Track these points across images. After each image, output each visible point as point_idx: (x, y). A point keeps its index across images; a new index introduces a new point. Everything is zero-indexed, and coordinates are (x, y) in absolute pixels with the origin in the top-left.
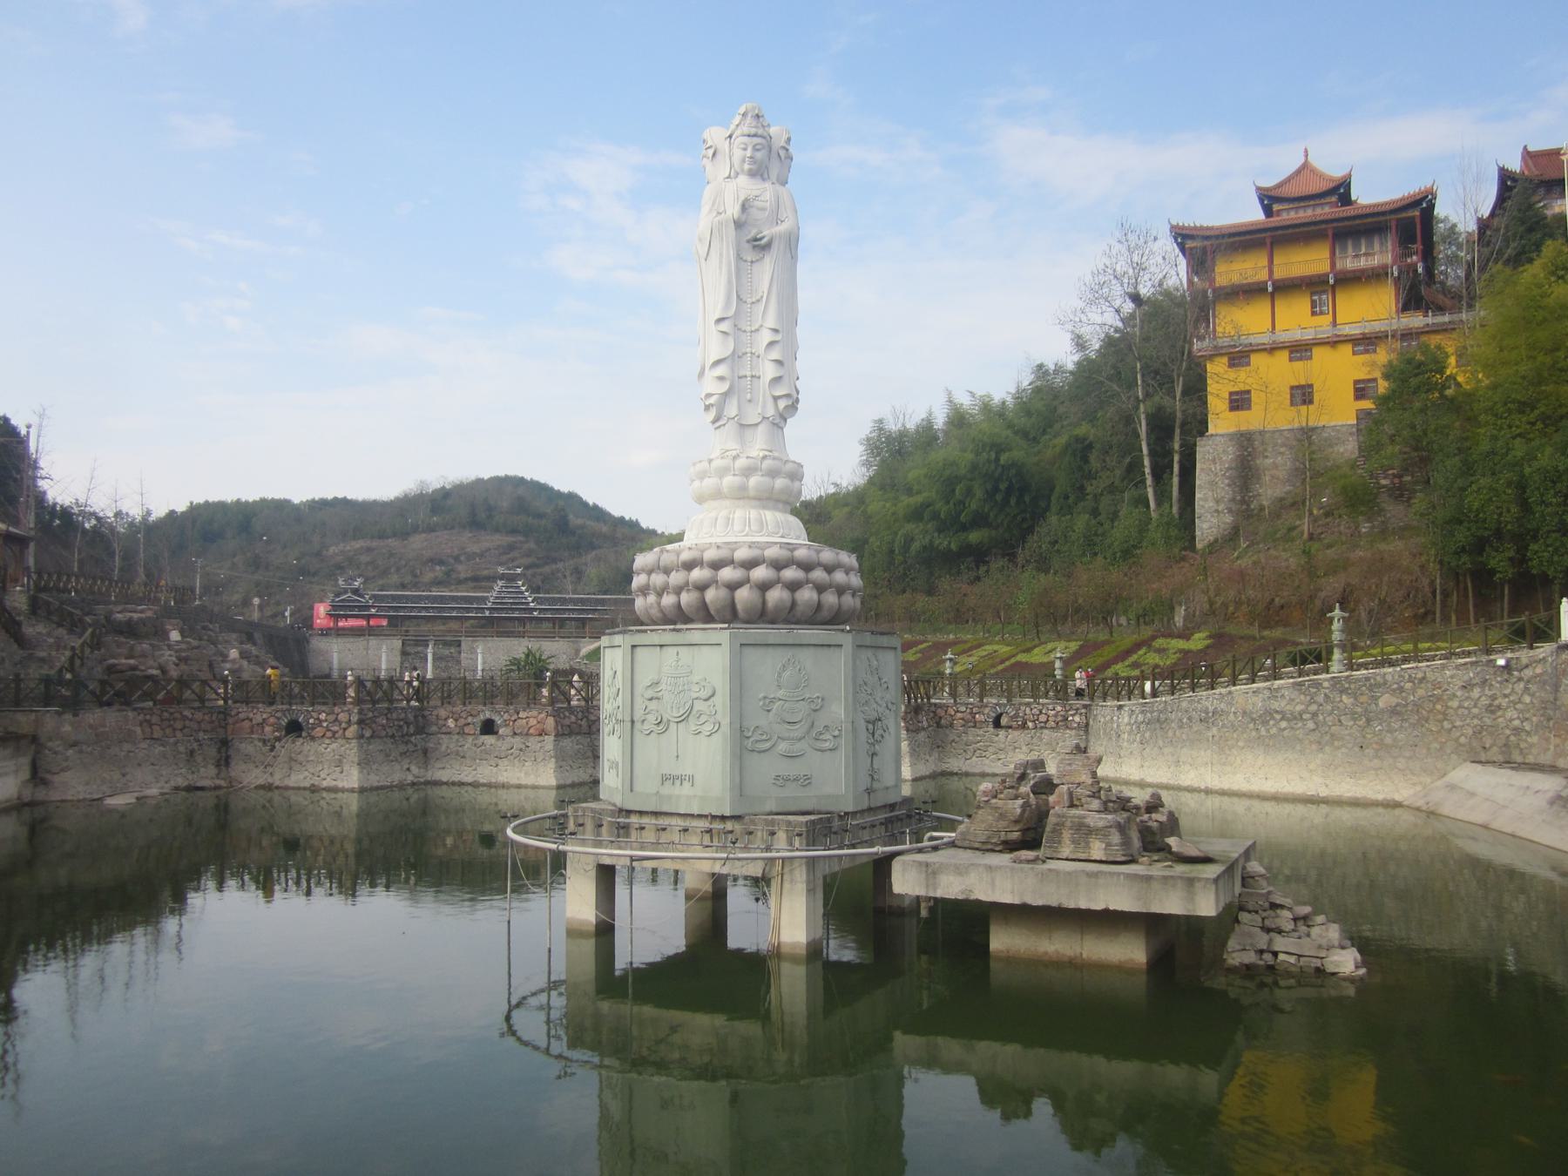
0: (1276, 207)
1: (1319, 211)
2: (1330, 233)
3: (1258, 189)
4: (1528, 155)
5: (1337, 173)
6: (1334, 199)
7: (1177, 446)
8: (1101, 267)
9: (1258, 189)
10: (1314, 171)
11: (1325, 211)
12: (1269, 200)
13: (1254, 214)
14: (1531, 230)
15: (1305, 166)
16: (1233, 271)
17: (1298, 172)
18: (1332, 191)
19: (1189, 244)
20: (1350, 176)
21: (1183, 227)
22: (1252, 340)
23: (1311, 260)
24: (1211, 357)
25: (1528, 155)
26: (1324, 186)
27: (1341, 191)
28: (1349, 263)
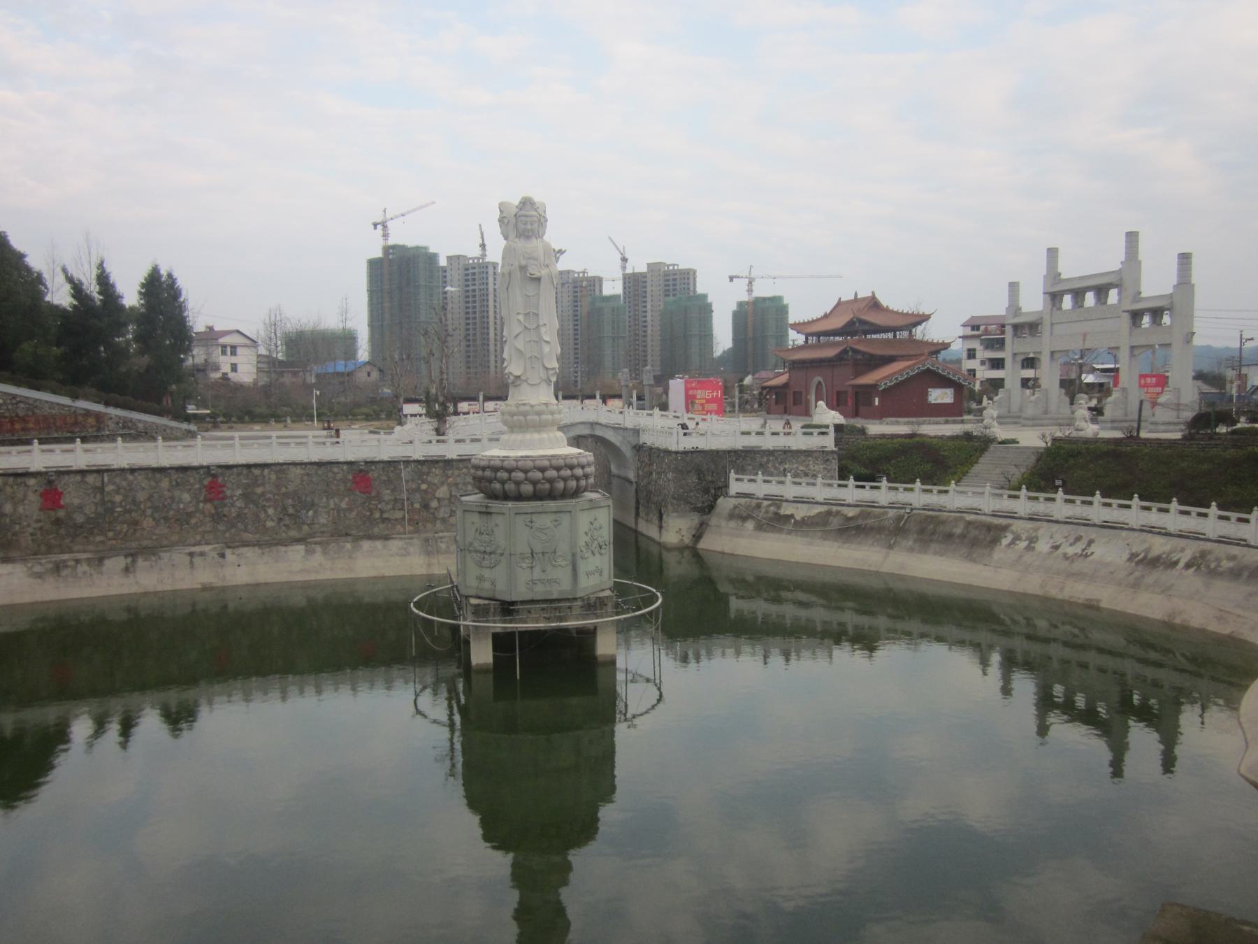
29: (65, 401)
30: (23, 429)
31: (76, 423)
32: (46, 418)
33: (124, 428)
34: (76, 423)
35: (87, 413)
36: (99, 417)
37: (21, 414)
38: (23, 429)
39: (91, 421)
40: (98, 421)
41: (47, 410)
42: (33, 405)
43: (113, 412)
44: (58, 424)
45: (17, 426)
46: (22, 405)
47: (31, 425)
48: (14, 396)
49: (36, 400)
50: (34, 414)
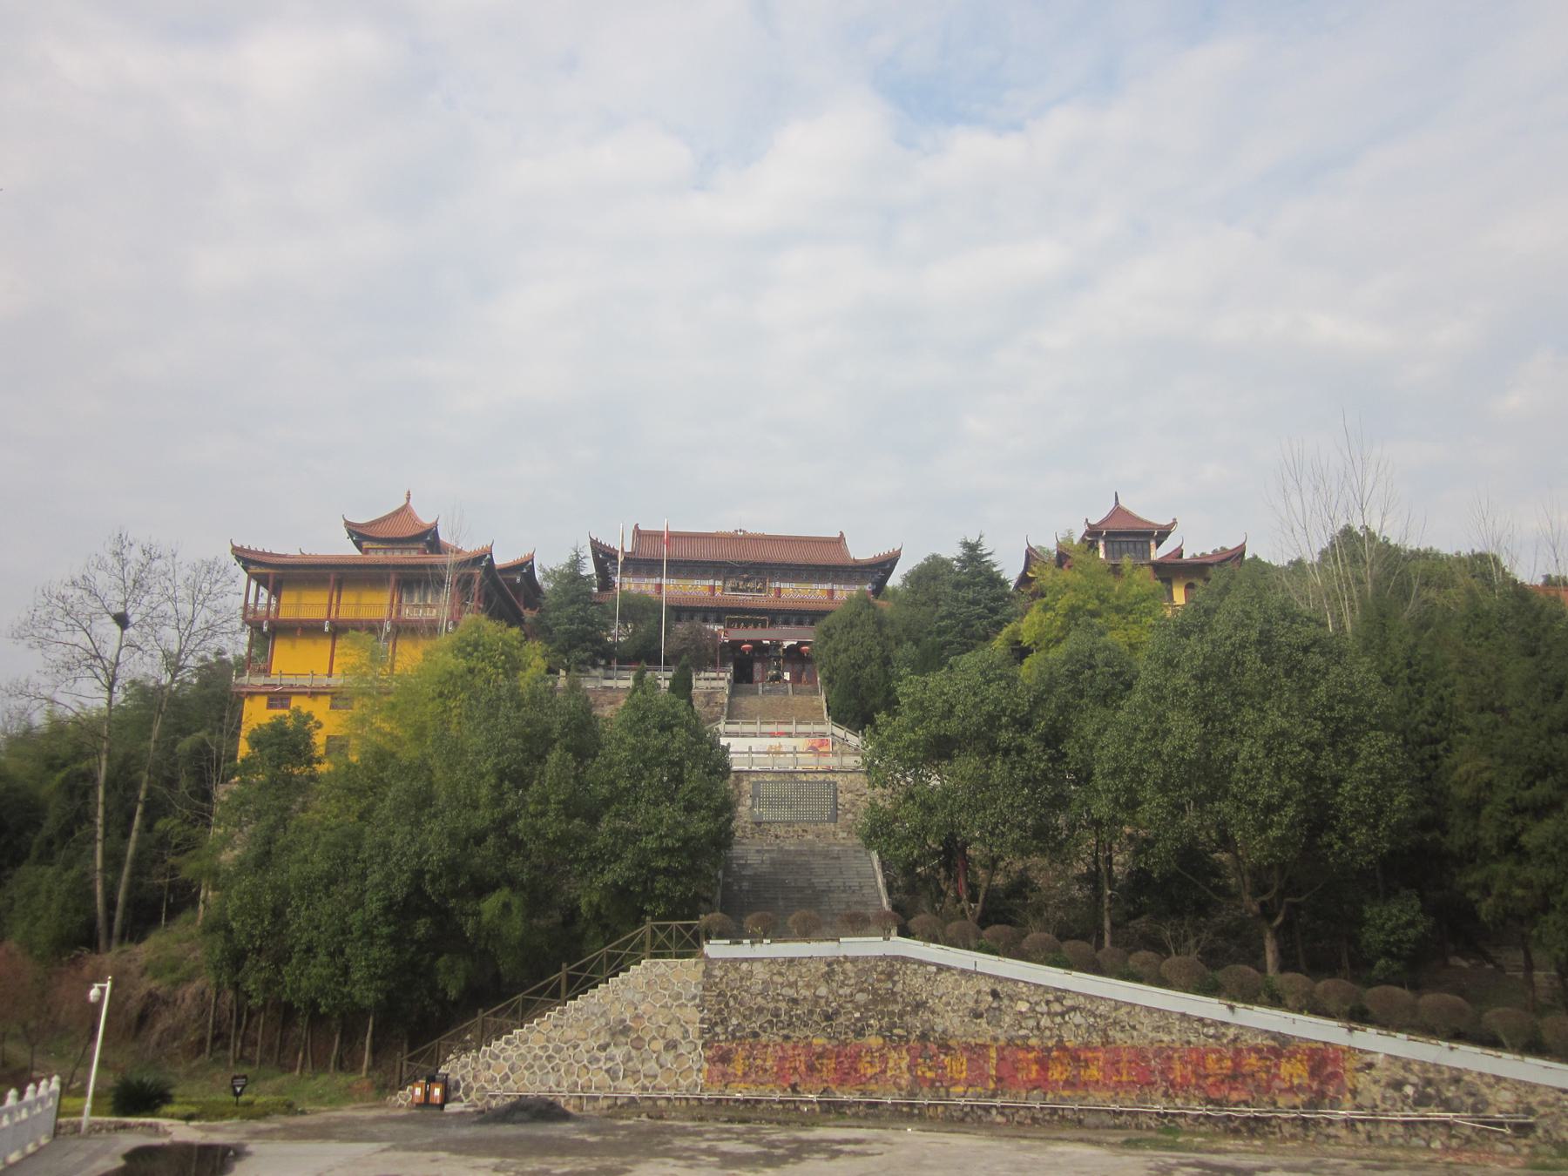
0: (365, 545)
1: (406, 554)
2: (393, 578)
3: (347, 524)
4: (639, 534)
5: (427, 520)
6: (421, 546)
7: (142, 796)
8: (78, 578)
9: (347, 524)
10: (411, 515)
11: (411, 556)
12: (358, 534)
13: (346, 549)
14: (572, 602)
15: (405, 509)
16: (310, 605)
17: (397, 513)
18: (419, 538)
19: (253, 569)
20: (436, 524)
21: (249, 551)
22: (291, 680)
23: (375, 604)
24: (251, 694)
25: (639, 534)
26: (418, 531)
27: (429, 539)
28: (407, 613)
29: (1210, 1008)
30: (1069, 1084)
31: (1235, 1077)
32: (1140, 1054)
33: (1422, 1100)
34: (1235, 1077)
35: (1281, 1047)
36: (1321, 1060)
37: (1071, 1042)
38: (1069, 1084)
39: (1293, 1071)
40: (1314, 1073)
41: (1146, 1035)
42: (1110, 1018)
43: (1370, 1040)
44: (1176, 1075)
45: (1056, 1074)
46: (1077, 1018)
47: (1094, 1073)
48: (1060, 994)
49: (1118, 1005)
50: (1107, 1041)
